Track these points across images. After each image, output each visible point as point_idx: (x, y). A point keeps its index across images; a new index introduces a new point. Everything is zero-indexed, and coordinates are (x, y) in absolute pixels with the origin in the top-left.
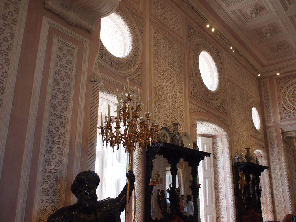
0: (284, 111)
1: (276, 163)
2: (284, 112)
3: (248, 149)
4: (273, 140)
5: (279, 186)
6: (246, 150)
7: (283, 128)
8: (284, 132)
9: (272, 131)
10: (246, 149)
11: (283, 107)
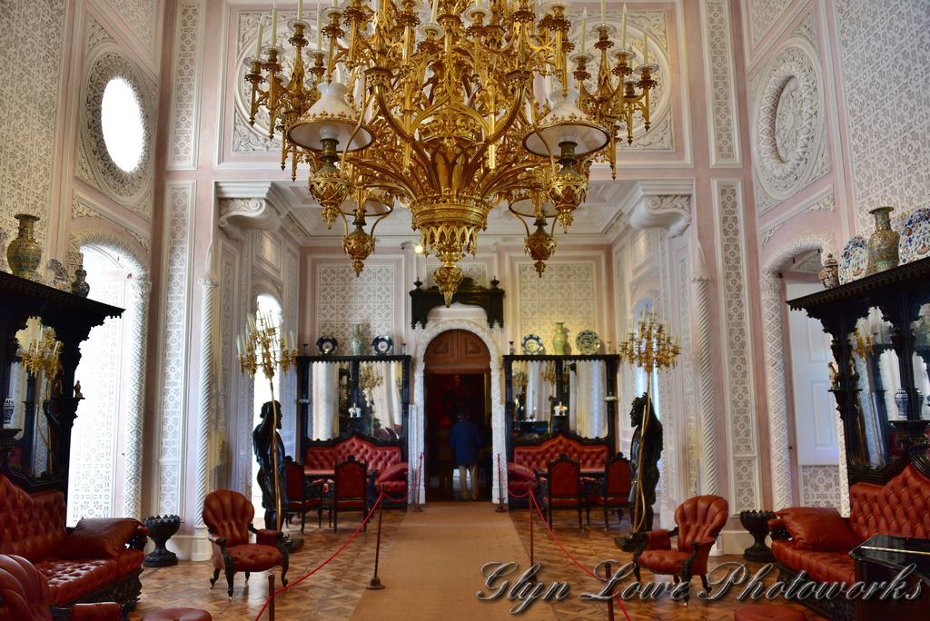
0: (235, 123)
1: (181, 304)
2: (235, 129)
3: (26, 220)
4: (184, 220)
5: (176, 384)
6: (18, 222)
7: (221, 185)
8: (226, 199)
9: (183, 188)
10: (17, 217)
11: (236, 111)
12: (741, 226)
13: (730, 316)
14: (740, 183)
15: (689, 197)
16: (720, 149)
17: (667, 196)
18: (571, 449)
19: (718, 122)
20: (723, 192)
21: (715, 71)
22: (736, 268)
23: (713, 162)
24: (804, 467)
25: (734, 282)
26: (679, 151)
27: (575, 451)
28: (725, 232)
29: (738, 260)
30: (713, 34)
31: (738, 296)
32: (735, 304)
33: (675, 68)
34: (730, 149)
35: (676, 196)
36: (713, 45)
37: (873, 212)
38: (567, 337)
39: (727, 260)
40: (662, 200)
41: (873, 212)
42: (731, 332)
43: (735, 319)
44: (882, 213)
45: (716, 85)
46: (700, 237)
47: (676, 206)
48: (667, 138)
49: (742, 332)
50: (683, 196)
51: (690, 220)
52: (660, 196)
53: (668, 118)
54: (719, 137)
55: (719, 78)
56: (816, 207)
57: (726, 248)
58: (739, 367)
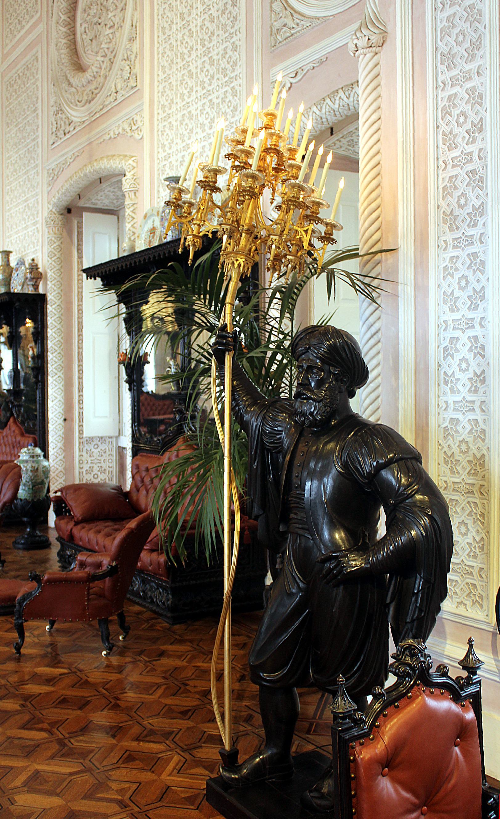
44: (7, 253)
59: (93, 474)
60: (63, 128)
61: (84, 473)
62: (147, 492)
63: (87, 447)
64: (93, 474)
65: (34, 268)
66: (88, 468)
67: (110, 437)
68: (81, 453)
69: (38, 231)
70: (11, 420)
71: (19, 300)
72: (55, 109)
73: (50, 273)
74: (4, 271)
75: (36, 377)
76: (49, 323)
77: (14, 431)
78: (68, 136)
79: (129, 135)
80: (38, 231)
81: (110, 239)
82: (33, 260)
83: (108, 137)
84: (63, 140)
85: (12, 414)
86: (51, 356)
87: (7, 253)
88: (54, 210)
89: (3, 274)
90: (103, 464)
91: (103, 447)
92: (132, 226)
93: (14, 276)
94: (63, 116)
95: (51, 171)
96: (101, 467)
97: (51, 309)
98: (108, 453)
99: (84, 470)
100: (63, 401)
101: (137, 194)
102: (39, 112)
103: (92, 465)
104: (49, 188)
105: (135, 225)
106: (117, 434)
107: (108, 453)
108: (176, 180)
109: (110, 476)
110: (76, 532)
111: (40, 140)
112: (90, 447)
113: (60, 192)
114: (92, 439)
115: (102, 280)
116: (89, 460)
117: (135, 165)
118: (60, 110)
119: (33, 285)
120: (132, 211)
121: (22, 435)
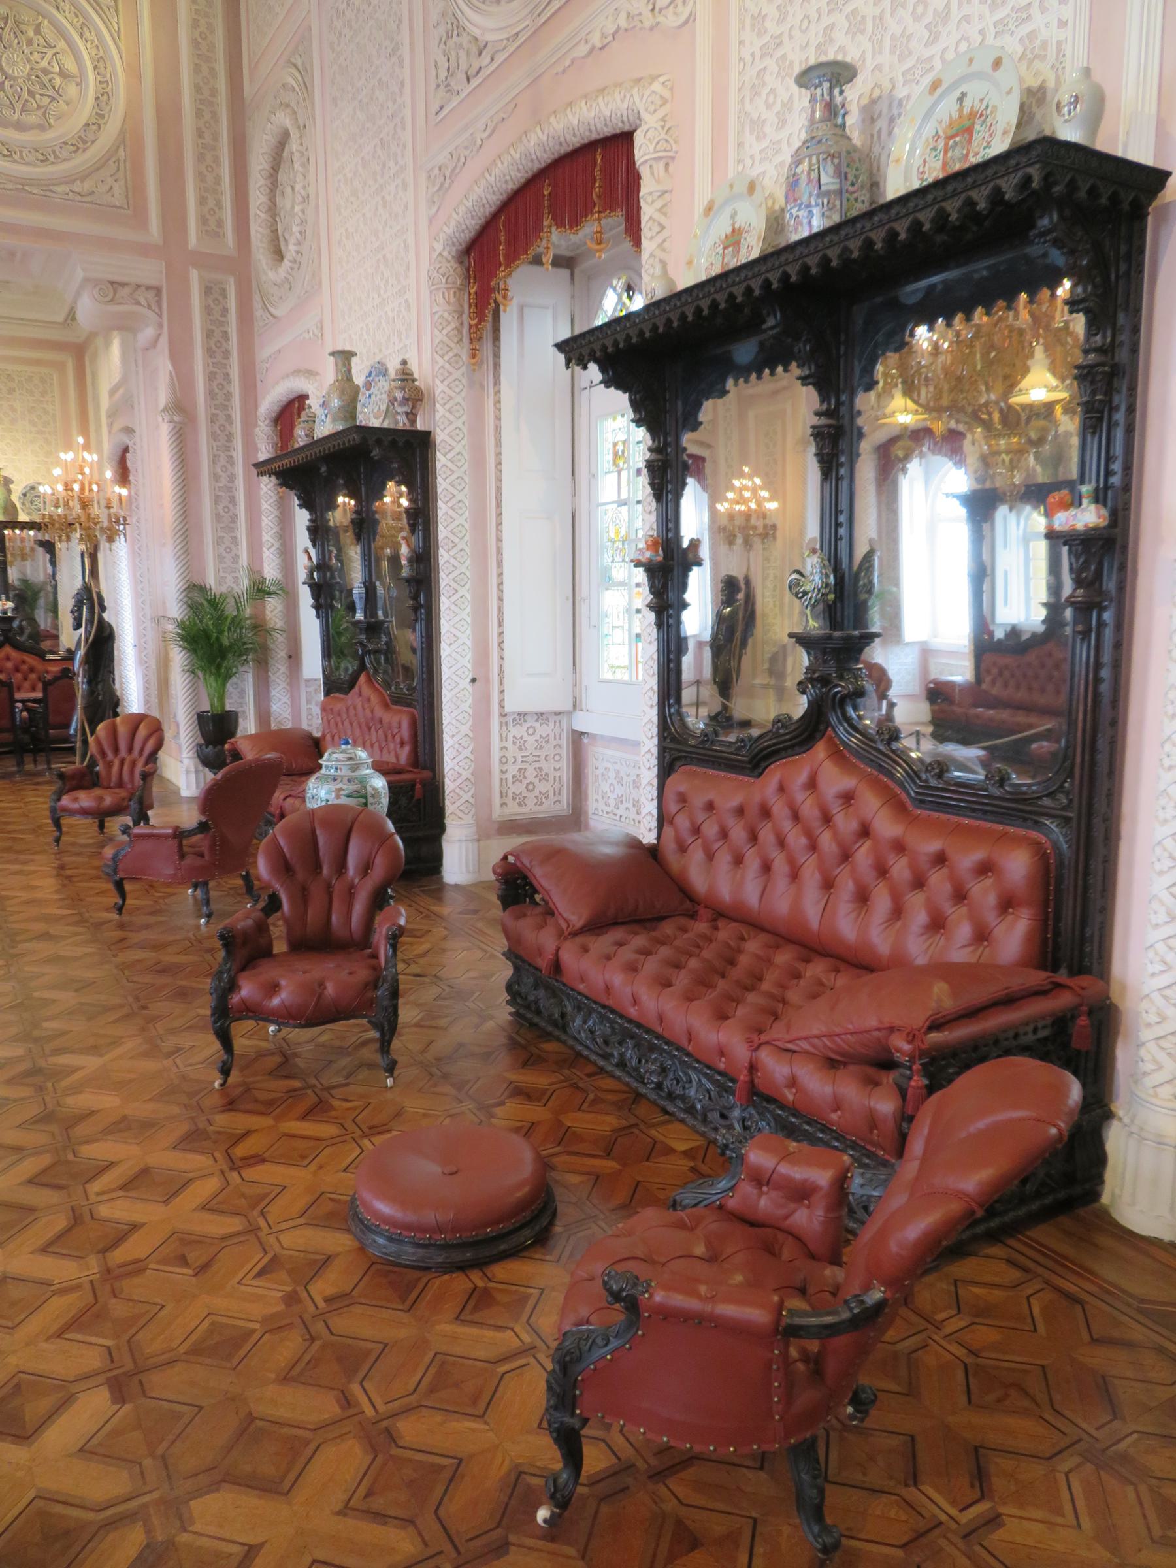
12: (234, 344)
13: (216, 477)
14: (232, 280)
15: (158, 291)
16: (203, 220)
17: (123, 285)
18: (25, 667)
19: (200, 177)
20: (207, 291)
21: (197, 89)
22: (226, 407)
23: (193, 241)
24: (307, 681)
25: (222, 428)
26: (139, 217)
27: (32, 670)
28: (210, 353)
29: (228, 396)
30: (195, 24)
31: (228, 449)
32: (223, 461)
33: (134, 72)
34: (220, 223)
35: (139, 286)
36: (195, 43)
37: (332, 354)
38: (9, 491)
39: (211, 395)
40: (115, 292)
41: (332, 354)
42: (217, 499)
43: (223, 482)
44: (345, 357)
45: (199, 114)
46: (173, 357)
47: (138, 303)
48: (118, 189)
49: (233, 501)
50: (148, 288)
51: (161, 326)
52: (112, 283)
53: (121, 152)
54: (202, 201)
55: (204, 105)
56: (307, 336)
57: (211, 377)
58: (228, 550)
59: (525, 782)
60: (464, 66)
61: (510, 781)
62: (710, 857)
63: (515, 731)
64: (525, 782)
65: (406, 376)
66: (516, 772)
67: (557, 714)
68: (504, 744)
69: (408, 308)
70: (362, 678)
71: (379, 442)
72: (442, 30)
73: (440, 389)
74: (343, 392)
75: (415, 597)
76: (439, 490)
77: (369, 700)
78: (475, 82)
79: (647, 24)
80: (408, 308)
81: (555, 318)
82: (404, 362)
83: (587, 48)
84: (462, 95)
85: (362, 667)
86: (445, 557)
87: (345, 357)
88: (445, 254)
89: (340, 398)
90: (543, 764)
91: (543, 730)
92: (660, 246)
93: (362, 398)
94: (464, 39)
95: (436, 171)
96: (541, 769)
97: (442, 461)
98: (553, 742)
99: (509, 776)
100: (469, 643)
101: (671, 168)
102: (406, 51)
103: (524, 766)
104: (434, 209)
105: (666, 245)
106: (568, 707)
107: (553, 742)
108: (837, 74)
109: (557, 786)
110: (568, 957)
111: (408, 112)
112: (518, 731)
113: (462, 209)
114: (523, 715)
115: (603, 370)
116: (519, 755)
117: (666, 94)
118: (456, 27)
119: (407, 414)
120: (660, 210)
121: (386, 706)
